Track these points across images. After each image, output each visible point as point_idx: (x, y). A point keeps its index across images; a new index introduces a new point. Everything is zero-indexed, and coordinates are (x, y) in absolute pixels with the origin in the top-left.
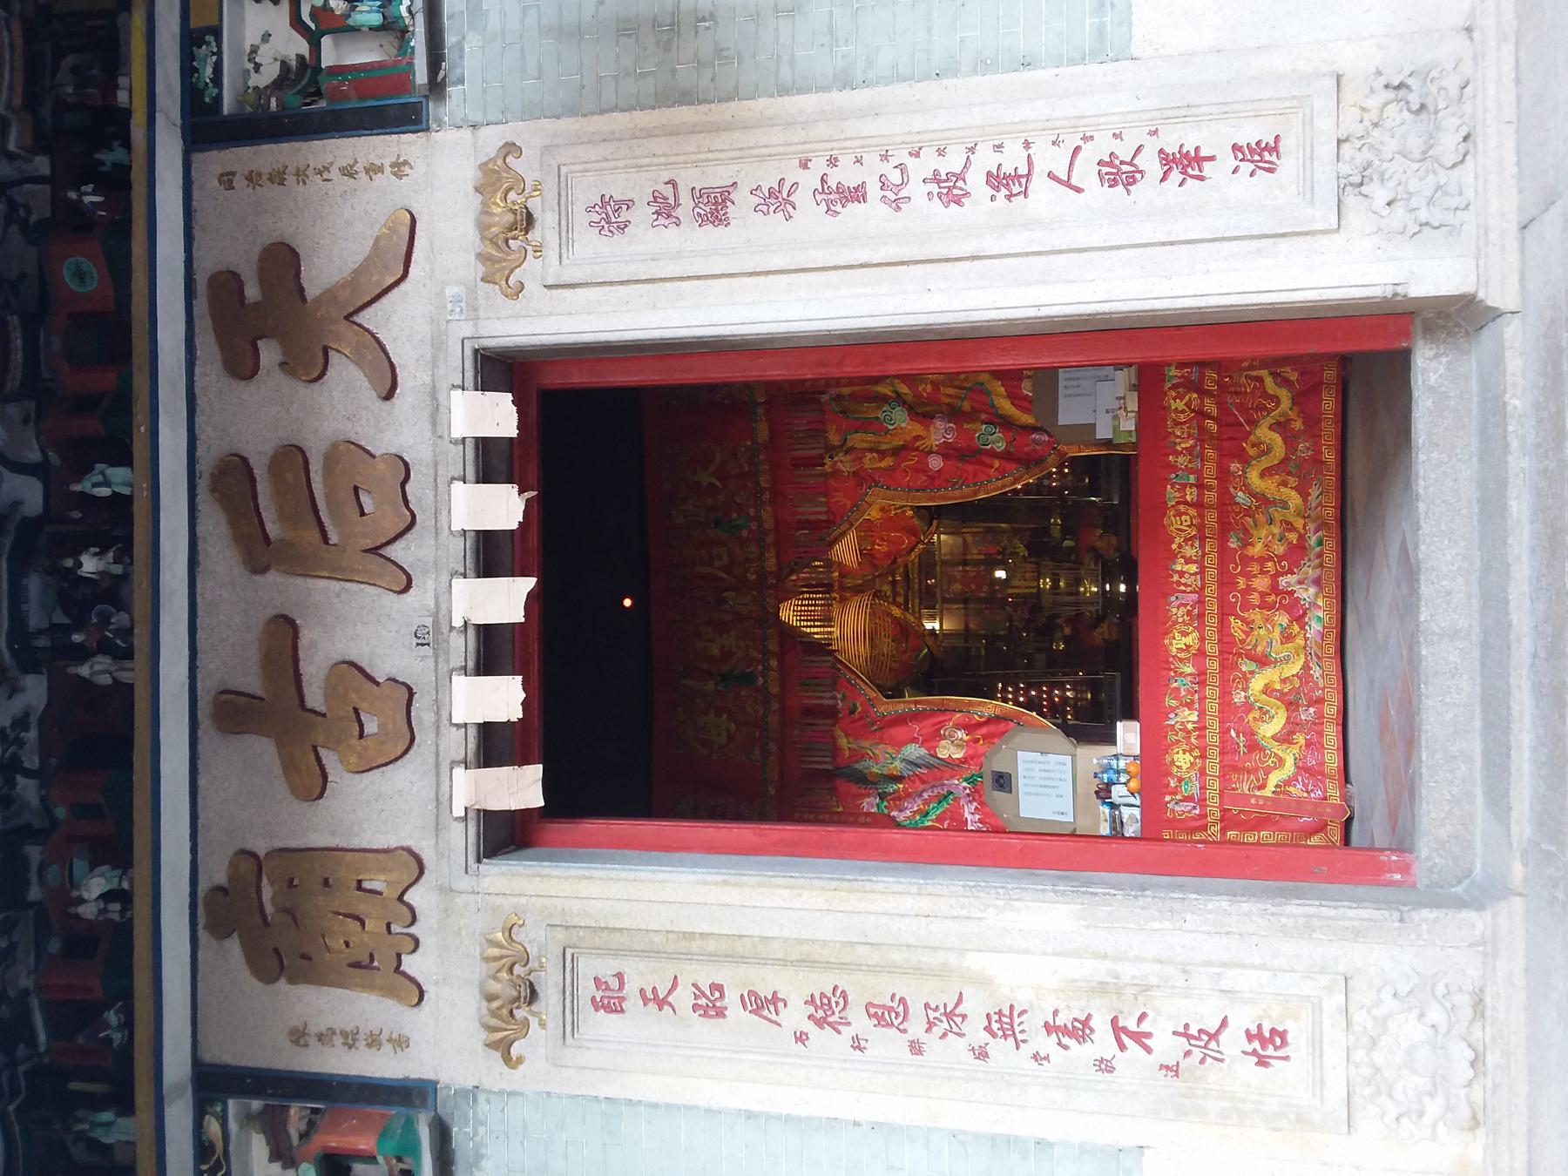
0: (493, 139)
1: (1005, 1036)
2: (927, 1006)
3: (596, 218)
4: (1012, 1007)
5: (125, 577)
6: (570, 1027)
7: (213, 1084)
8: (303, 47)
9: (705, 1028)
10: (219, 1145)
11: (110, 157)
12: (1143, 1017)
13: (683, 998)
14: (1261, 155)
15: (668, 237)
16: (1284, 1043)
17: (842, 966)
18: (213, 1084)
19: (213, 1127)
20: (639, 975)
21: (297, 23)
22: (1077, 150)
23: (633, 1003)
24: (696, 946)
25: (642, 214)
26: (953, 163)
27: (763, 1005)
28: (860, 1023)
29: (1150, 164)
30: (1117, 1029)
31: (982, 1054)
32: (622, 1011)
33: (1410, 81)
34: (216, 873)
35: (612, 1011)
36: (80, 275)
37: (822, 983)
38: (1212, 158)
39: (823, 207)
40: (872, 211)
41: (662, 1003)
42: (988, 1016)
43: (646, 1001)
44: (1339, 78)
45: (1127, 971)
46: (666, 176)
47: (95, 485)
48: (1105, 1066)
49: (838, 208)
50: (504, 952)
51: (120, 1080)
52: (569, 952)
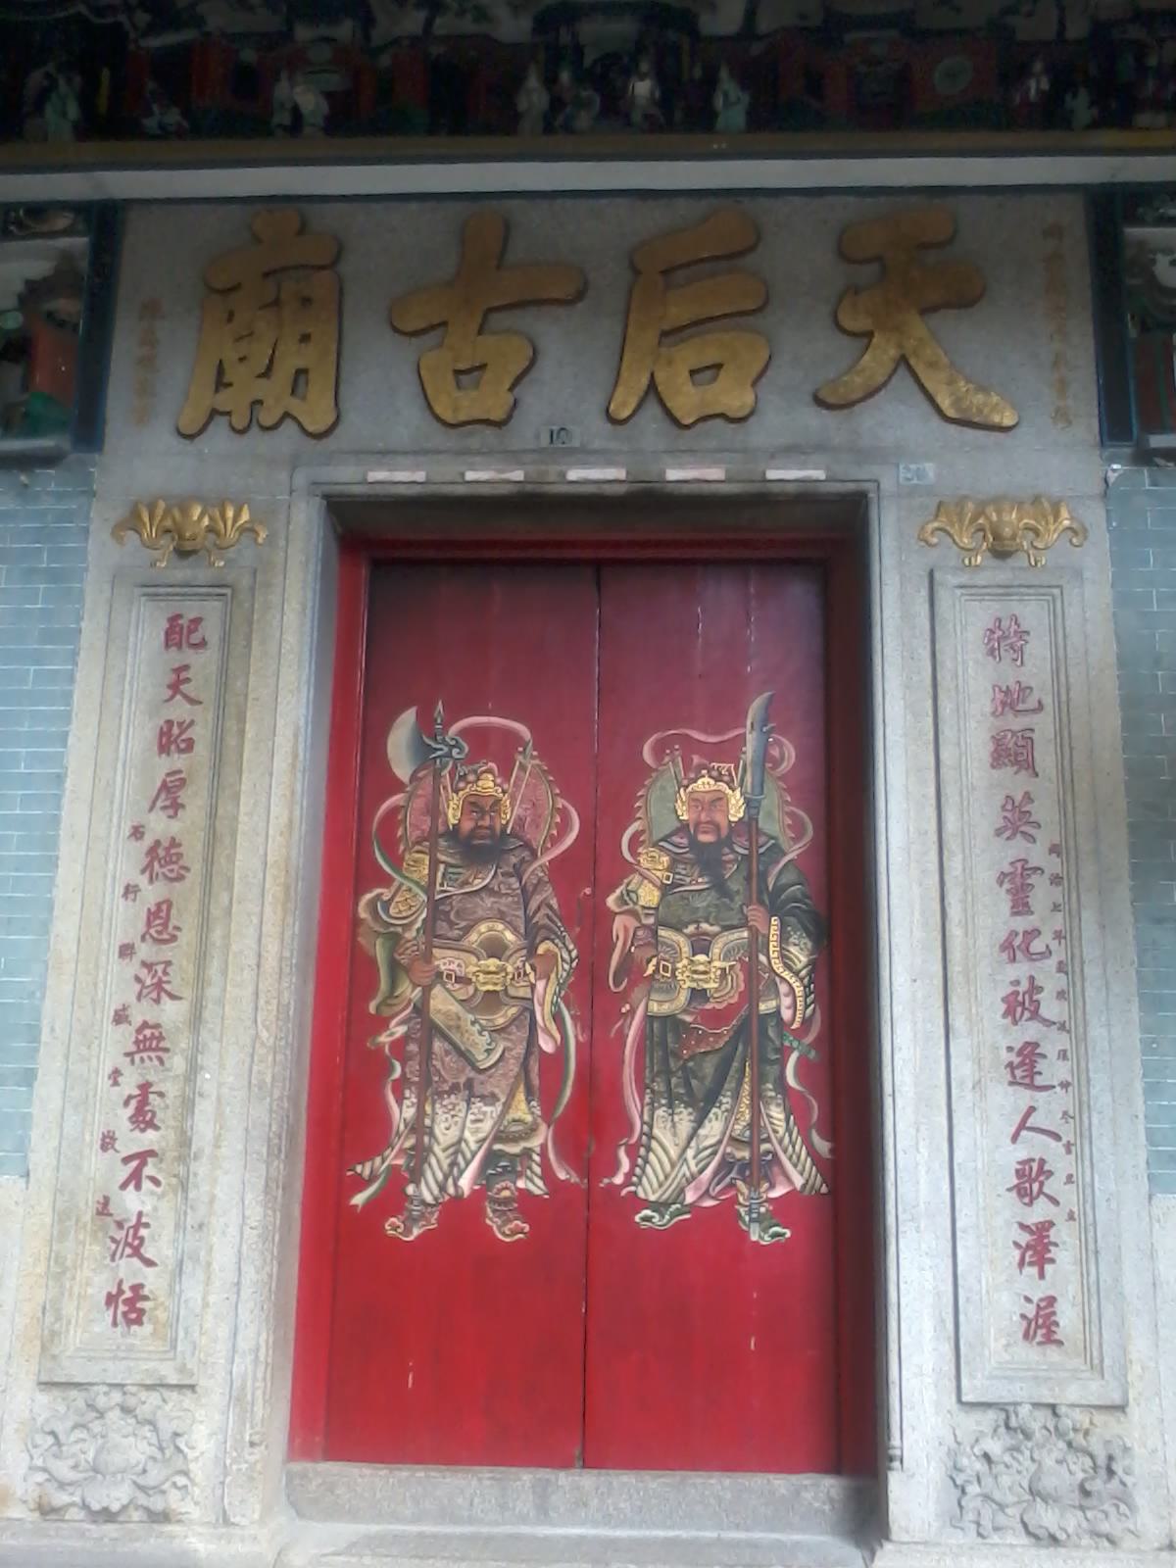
1: (137, 1042)
2: (168, 963)
3: (1005, 624)
4: (166, 1050)
5: (628, 123)
6: (153, 589)
10: (45, 228)
11: (1080, 104)
12: (155, 1181)
13: (180, 710)
14: (1041, 1325)
16: (130, 1322)
17: (208, 877)
18: (104, 221)
19: (62, 222)
22: (1057, 1137)
23: (176, 658)
24: (231, 725)
25: (1010, 676)
26: (1050, 1008)
27: (170, 794)
28: (151, 893)
29: (1040, 1211)
30: (143, 1157)
32: (167, 645)
33: (1115, 1482)
35: (167, 634)
37: (193, 853)
38: (1042, 1275)
39: (1007, 869)
41: (175, 687)
42: (157, 1026)
43: (178, 671)
44: (1121, 1408)
45: (200, 1168)
46: (1048, 701)
47: (726, 95)
48: (108, 1142)
49: (1006, 886)
50: (230, 523)
52: (227, 591)
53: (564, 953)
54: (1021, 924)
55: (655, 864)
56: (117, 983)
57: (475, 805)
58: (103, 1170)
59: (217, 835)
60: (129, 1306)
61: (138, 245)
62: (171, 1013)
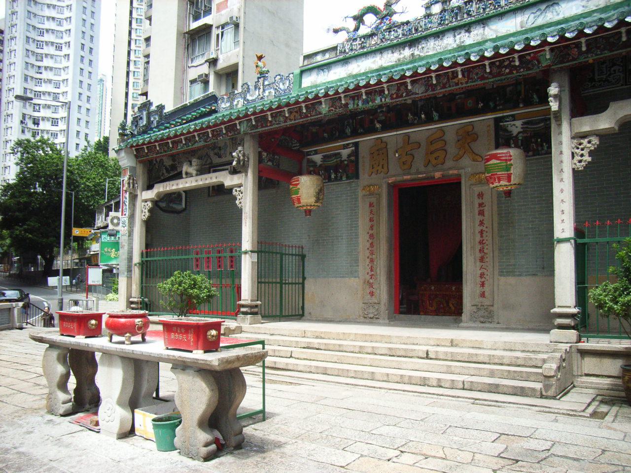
8: (515, 133)
9: (368, 219)
14: (483, 295)
20: (374, 209)
21: (519, 133)
25: (480, 201)
26: (485, 251)
27: (372, 227)
28: (371, 241)
30: (372, 275)
31: (368, 258)
34: (384, 140)
36: (470, 103)
51: (355, 133)
54: (481, 239)
56: (367, 253)
58: (368, 277)
59: (378, 233)
61: (361, 148)
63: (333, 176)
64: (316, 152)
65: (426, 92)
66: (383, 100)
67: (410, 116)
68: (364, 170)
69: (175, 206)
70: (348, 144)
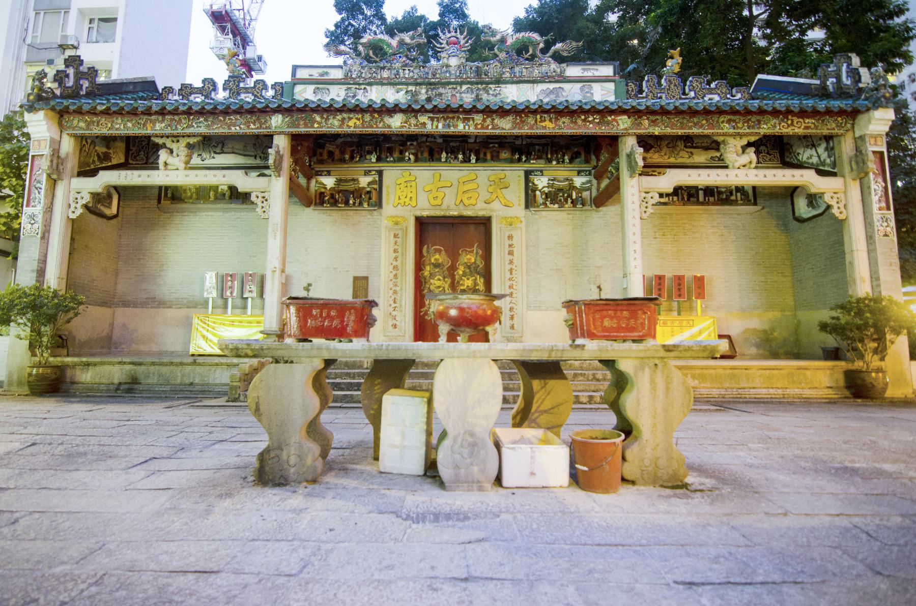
0: (523, 219)
7: (380, 173)
9: (392, 250)
15: (507, 246)
20: (399, 240)
27: (396, 259)
28: (394, 272)
40: (508, 275)
53: (449, 281)
55: (462, 268)
57: (436, 259)
58: (391, 309)
60: (395, 326)
62: (398, 289)
63: (351, 202)
64: (329, 173)
65: (514, 128)
66: (467, 127)
67: (444, 155)
68: (388, 199)
69: (102, 208)
70: (370, 171)
